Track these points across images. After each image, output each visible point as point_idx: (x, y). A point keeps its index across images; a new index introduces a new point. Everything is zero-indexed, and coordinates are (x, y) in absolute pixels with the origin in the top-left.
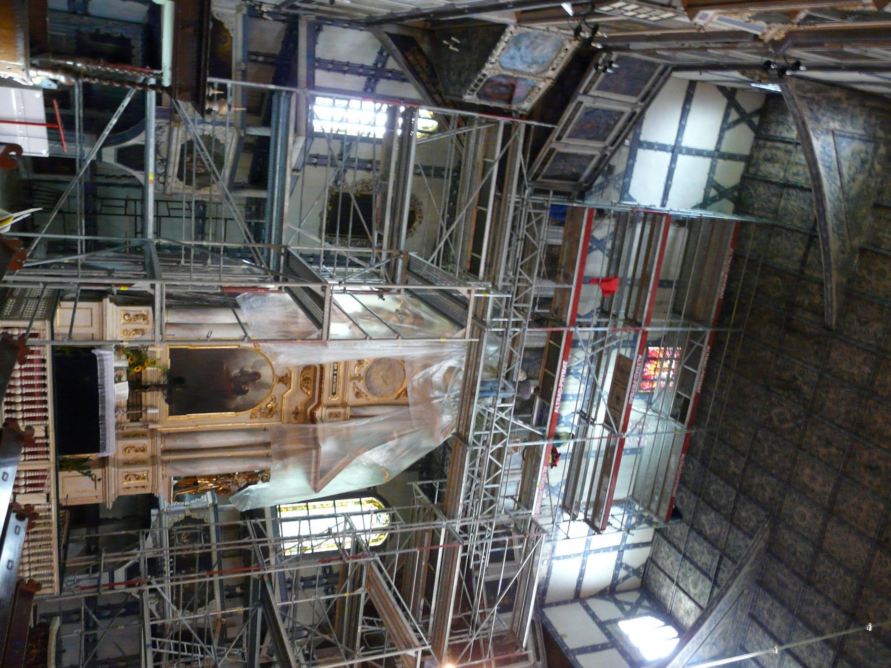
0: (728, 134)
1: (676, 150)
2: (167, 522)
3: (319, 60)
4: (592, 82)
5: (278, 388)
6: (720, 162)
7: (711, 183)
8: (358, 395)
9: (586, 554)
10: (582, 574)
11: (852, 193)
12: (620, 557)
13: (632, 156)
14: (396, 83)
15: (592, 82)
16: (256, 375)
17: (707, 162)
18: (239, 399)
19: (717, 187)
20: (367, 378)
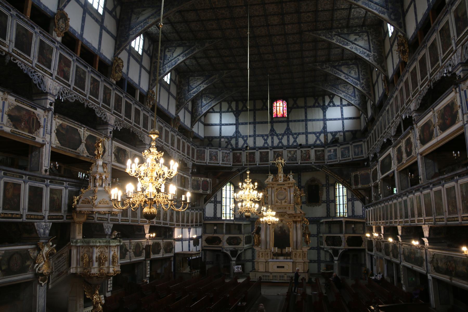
0: (216, 110)
1: (221, 125)
2: (326, 246)
3: (214, 216)
4: (203, 163)
5: (284, 222)
6: (222, 110)
7: (228, 111)
8: (285, 202)
9: (343, 119)
10: (350, 118)
11: (214, 97)
12: (345, 106)
13: (223, 137)
14: (217, 197)
15: (203, 163)
16: (281, 227)
17: (223, 114)
18: (286, 231)
19: (228, 109)
20: (281, 200)
